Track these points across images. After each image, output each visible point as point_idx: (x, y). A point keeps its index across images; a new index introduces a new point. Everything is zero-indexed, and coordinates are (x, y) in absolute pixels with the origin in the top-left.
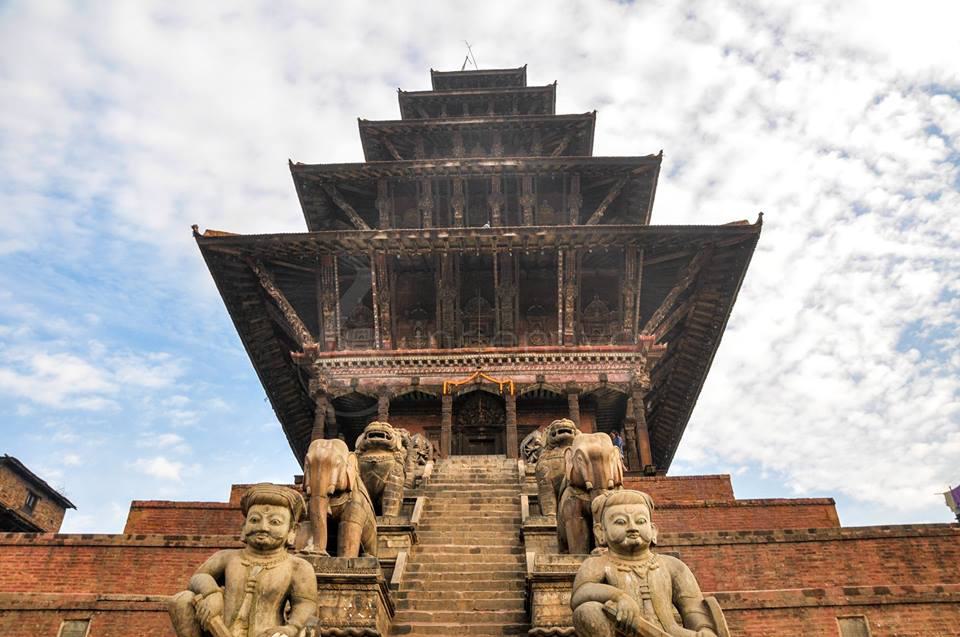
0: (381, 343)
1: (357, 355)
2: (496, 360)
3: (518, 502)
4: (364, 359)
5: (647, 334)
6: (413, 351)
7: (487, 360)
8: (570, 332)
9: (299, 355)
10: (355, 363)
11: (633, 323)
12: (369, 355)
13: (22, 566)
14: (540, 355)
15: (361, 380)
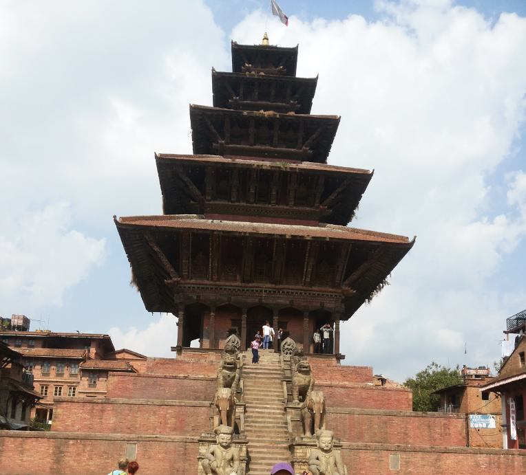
0: (212, 278)
1: (200, 284)
2: (270, 292)
3: (282, 384)
4: (203, 286)
5: (346, 285)
6: (227, 284)
7: (265, 291)
8: (308, 280)
9: (169, 281)
10: (198, 288)
11: (341, 278)
12: (206, 285)
13: (81, 411)
14: (293, 291)
15: (202, 298)
